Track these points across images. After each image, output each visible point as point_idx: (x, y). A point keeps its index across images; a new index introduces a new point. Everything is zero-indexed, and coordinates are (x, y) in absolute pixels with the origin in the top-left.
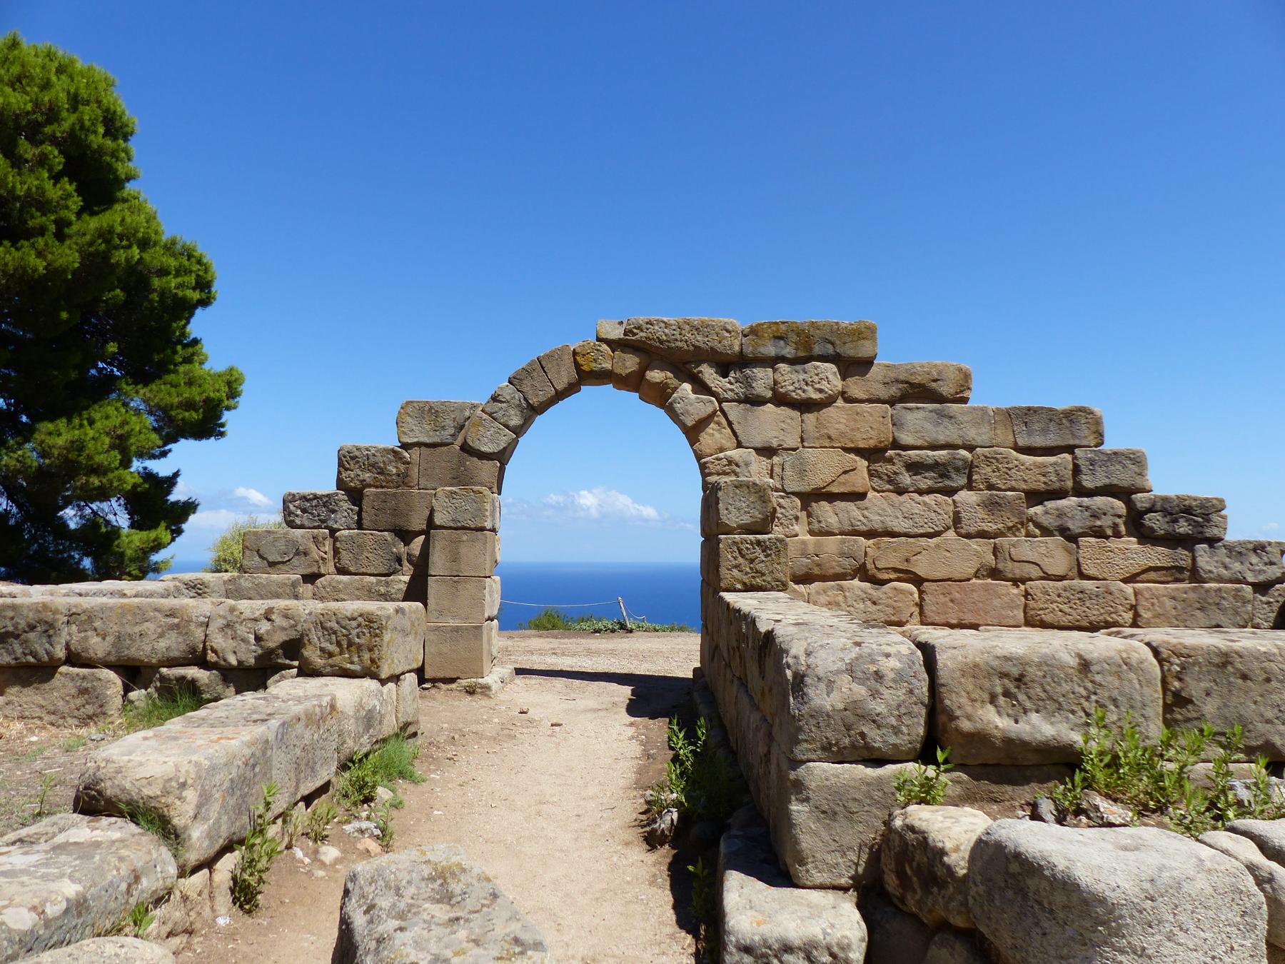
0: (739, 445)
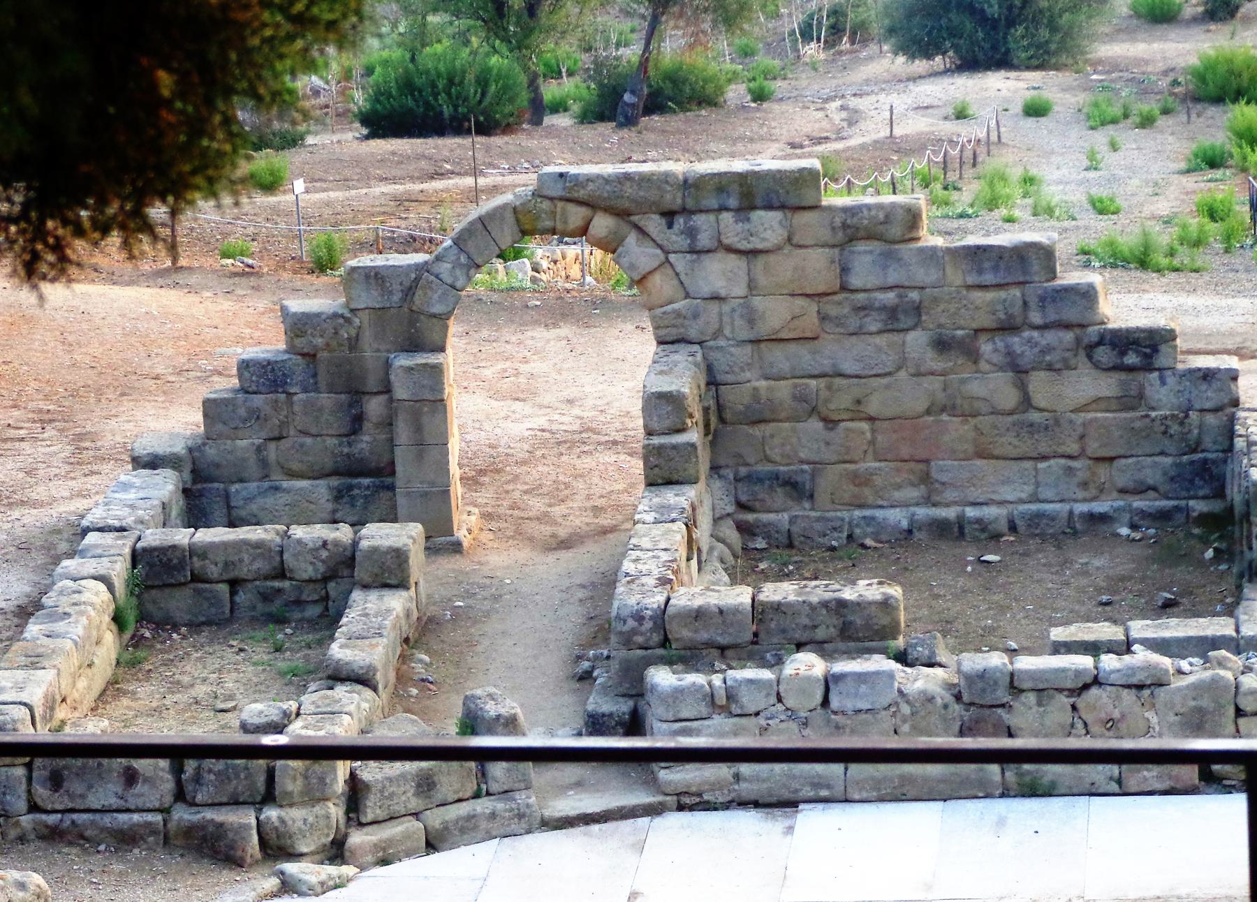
0: (687, 296)
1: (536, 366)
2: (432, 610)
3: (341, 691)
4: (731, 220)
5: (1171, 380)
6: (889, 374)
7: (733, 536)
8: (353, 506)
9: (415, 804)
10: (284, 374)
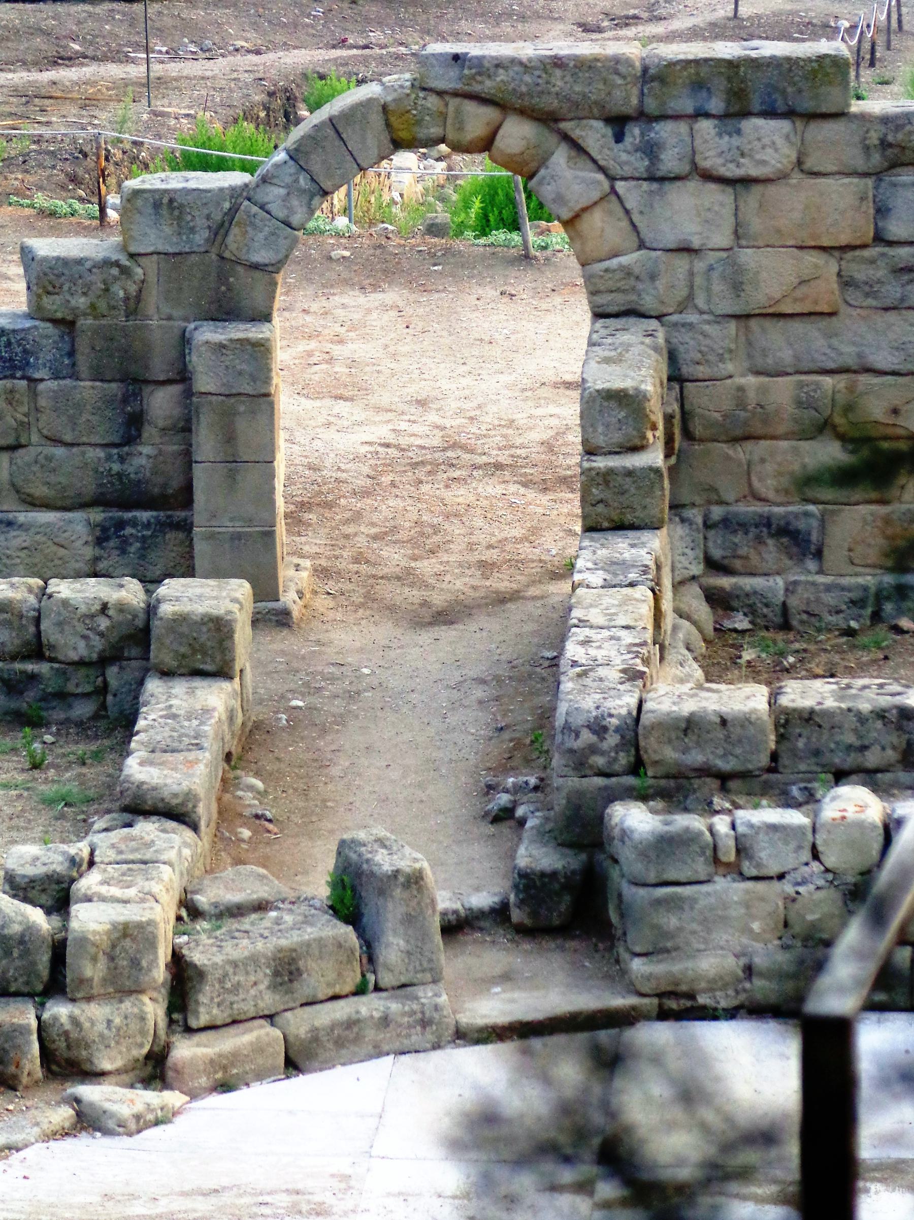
0: (642, 245)
1: (355, 348)
2: (258, 713)
3: (147, 828)
4: (713, 132)
7: (703, 611)
8: (123, 552)
9: (269, 1001)
10: (25, 351)
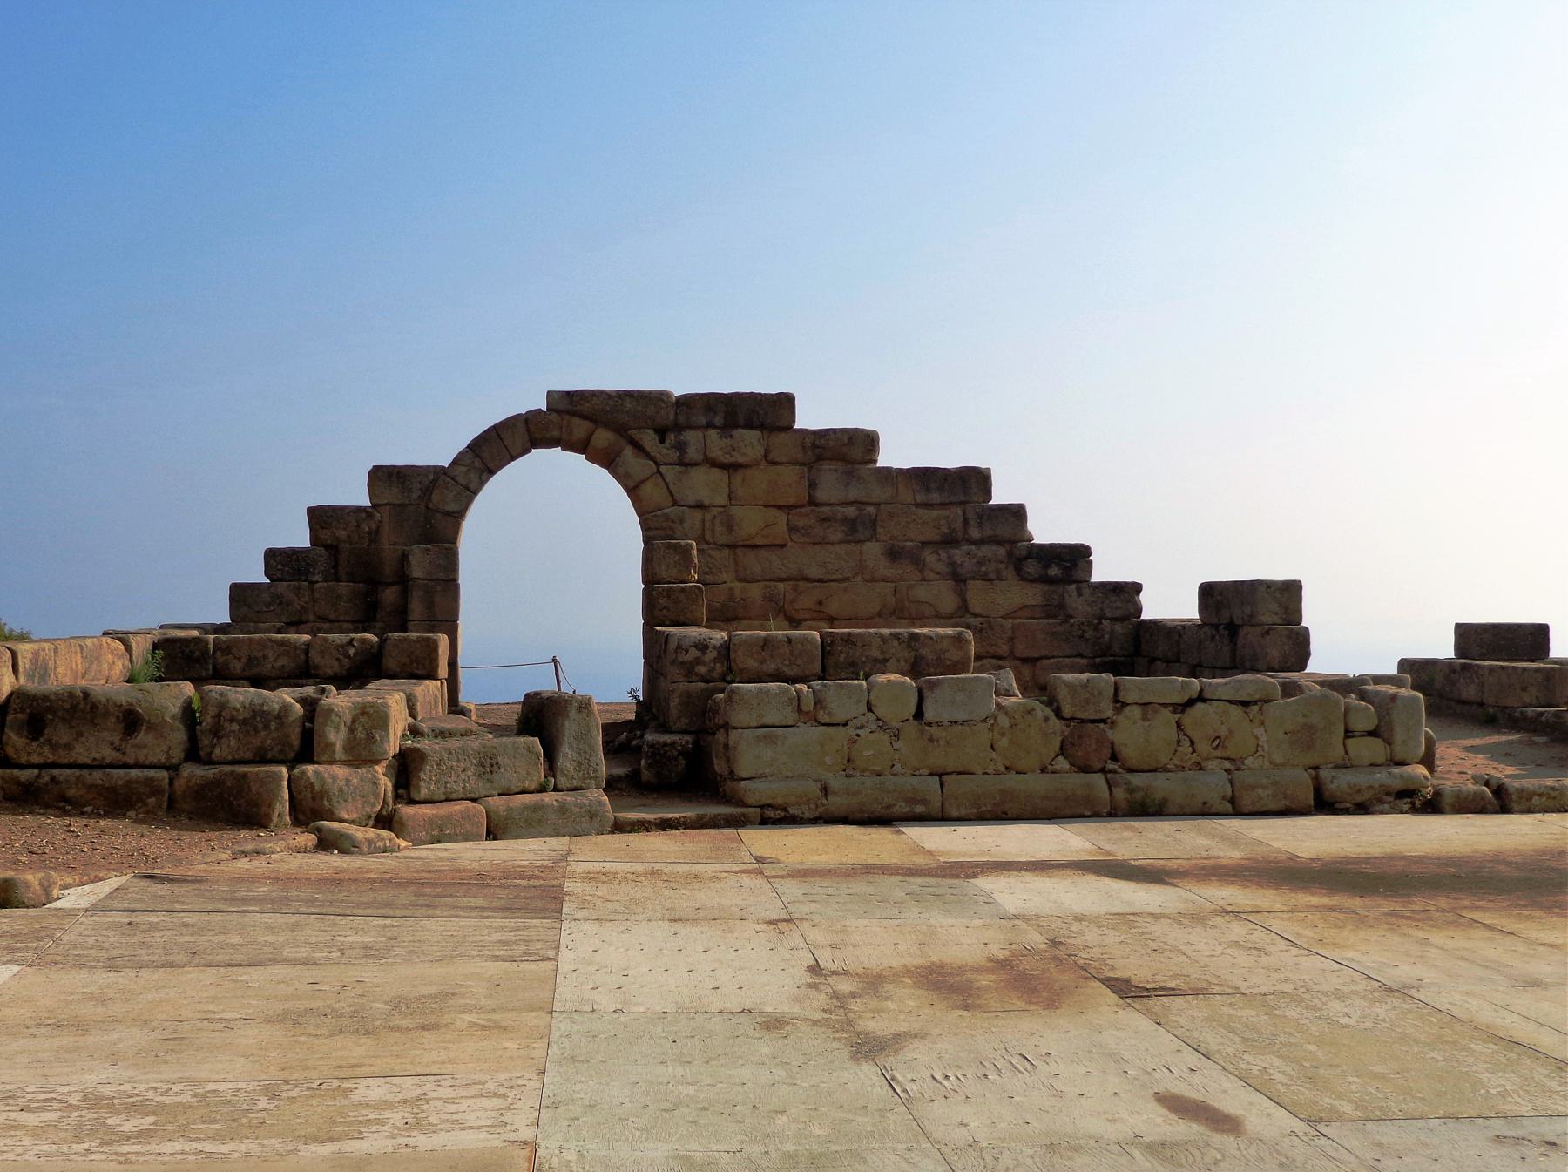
0: (675, 504)
5: (1087, 592)
6: (848, 579)
9: (476, 786)
